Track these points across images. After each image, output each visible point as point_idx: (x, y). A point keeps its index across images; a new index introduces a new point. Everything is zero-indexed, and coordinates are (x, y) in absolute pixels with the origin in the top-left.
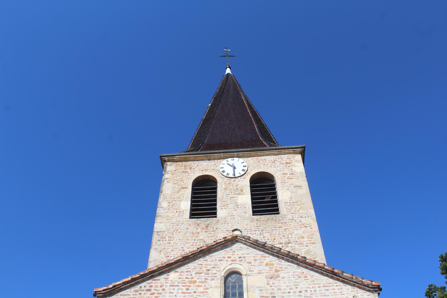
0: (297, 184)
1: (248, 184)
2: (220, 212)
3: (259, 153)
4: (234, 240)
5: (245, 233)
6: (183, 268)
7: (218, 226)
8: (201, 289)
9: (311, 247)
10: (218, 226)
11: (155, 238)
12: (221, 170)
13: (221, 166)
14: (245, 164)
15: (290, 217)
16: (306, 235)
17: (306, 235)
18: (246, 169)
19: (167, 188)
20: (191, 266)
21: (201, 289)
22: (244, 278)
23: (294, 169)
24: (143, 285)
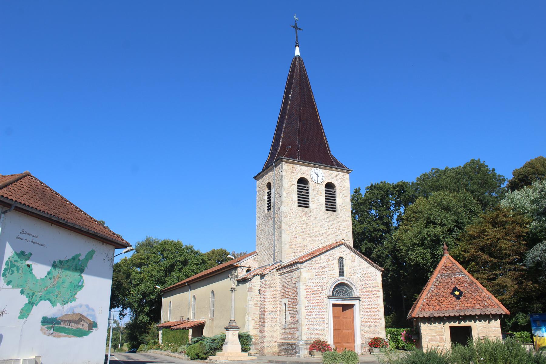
0: (345, 195)
1: (324, 189)
2: (311, 205)
3: (330, 168)
4: (342, 244)
5: (346, 242)
6: (326, 254)
7: (311, 214)
8: (332, 263)
9: (348, 233)
10: (311, 214)
11: (283, 216)
12: (312, 176)
13: (312, 173)
14: (323, 174)
15: (341, 215)
16: (347, 226)
17: (347, 226)
18: (323, 178)
19: (285, 182)
20: (328, 253)
21: (332, 263)
22: (344, 260)
23: (345, 183)
24: (313, 259)
